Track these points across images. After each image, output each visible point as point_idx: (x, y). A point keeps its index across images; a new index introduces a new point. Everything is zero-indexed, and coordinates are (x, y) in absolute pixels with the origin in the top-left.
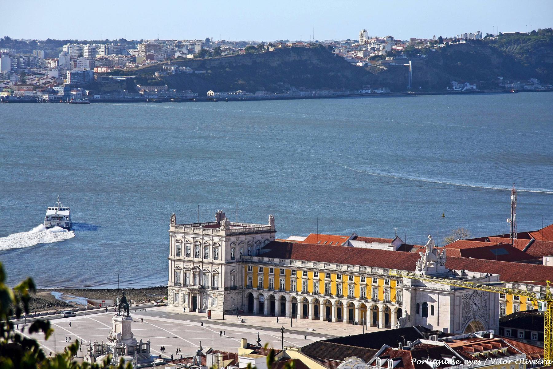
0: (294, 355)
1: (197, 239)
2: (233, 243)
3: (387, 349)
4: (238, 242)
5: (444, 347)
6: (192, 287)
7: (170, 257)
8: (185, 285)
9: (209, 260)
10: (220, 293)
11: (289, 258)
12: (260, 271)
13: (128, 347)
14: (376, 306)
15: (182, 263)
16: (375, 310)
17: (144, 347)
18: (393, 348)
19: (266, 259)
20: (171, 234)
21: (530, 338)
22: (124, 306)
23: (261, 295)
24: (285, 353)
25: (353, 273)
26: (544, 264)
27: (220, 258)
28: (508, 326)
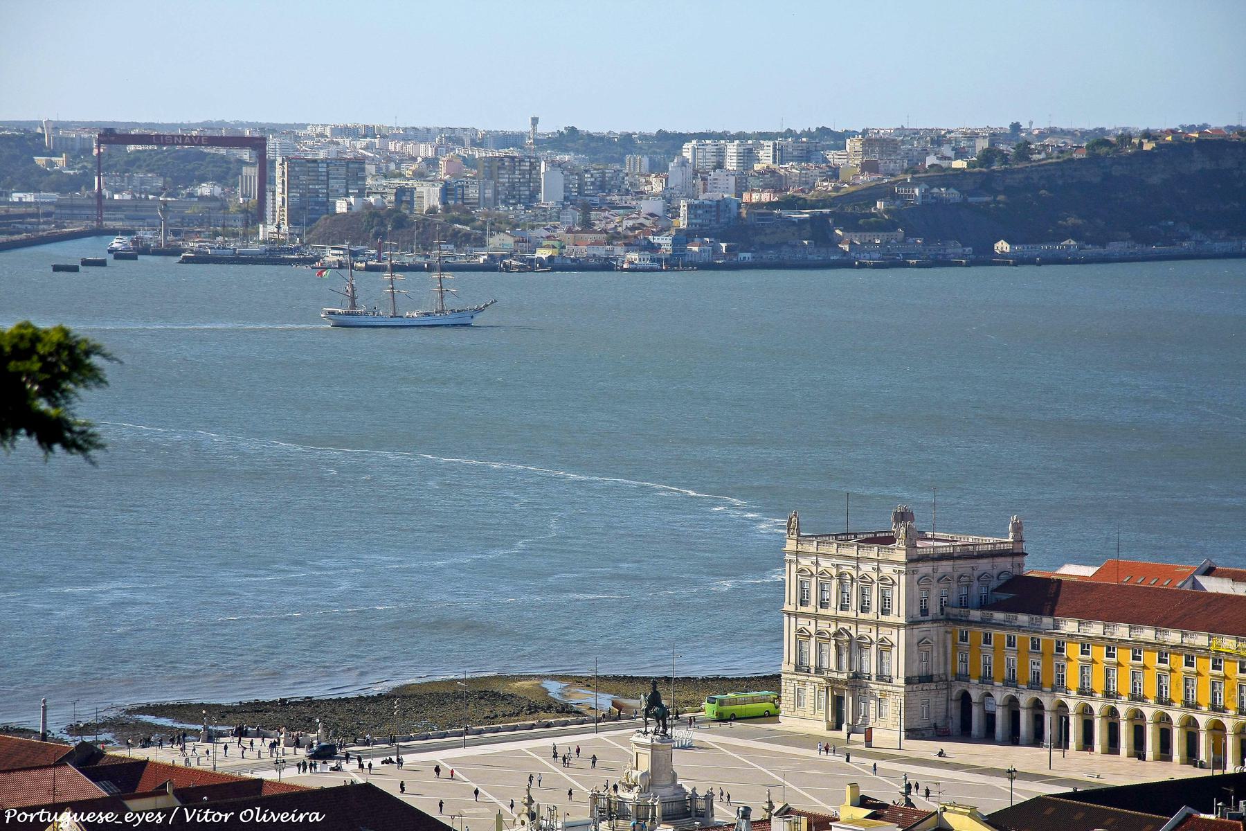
1: (844, 569)
2: (924, 580)
3: (1189, 816)
4: (939, 575)
6: (834, 675)
7: (787, 607)
8: (819, 670)
9: (871, 616)
10: (895, 689)
11: (1051, 614)
12: (985, 642)
13: (663, 802)
15: (813, 622)
16: (1191, 728)
17: (701, 804)
18: (1202, 815)
19: (999, 616)
20: (788, 557)
22: (658, 712)
23: (990, 695)
24: (940, 818)
25: (1194, 649)
27: (895, 612)
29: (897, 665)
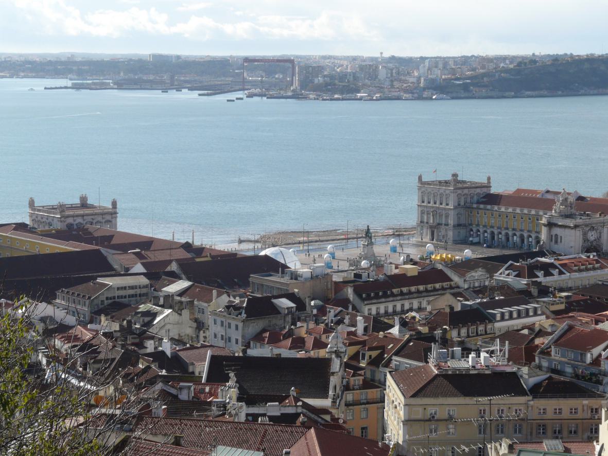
0: (440, 267)
3: (512, 264)
14: (538, 236)
17: (382, 263)
18: (516, 264)
19: (482, 206)
27: (450, 205)
29: (451, 222)
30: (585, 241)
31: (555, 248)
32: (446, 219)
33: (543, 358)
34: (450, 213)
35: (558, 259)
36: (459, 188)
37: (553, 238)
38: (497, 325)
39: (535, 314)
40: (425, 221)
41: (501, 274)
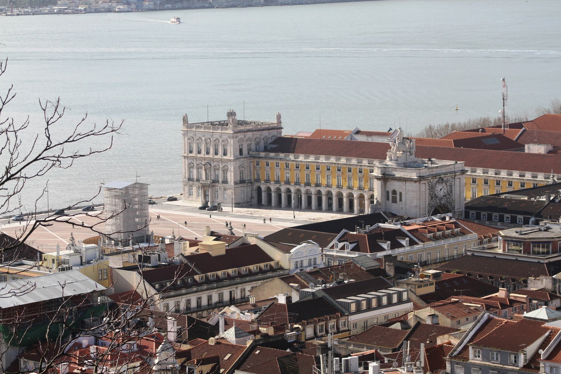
0: (252, 241)
3: (346, 233)
4: (247, 138)
5: (399, 230)
18: (351, 233)
19: (272, 155)
21: (503, 221)
24: (243, 239)
26: (526, 151)
27: (229, 154)
28: (484, 211)
29: (231, 177)
30: (432, 198)
31: (395, 208)
32: (224, 174)
33: (457, 364)
34: (229, 167)
35: (405, 224)
36: (240, 132)
37: (390, 195)
38: (353, 318)
39: (400, 301)
40: (195, 177)
41: (332, 247)
